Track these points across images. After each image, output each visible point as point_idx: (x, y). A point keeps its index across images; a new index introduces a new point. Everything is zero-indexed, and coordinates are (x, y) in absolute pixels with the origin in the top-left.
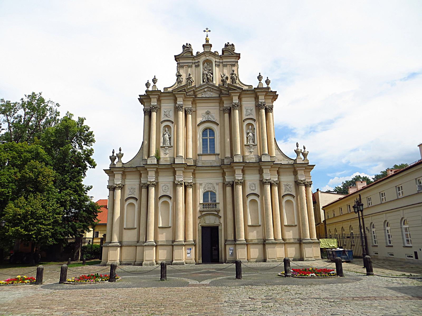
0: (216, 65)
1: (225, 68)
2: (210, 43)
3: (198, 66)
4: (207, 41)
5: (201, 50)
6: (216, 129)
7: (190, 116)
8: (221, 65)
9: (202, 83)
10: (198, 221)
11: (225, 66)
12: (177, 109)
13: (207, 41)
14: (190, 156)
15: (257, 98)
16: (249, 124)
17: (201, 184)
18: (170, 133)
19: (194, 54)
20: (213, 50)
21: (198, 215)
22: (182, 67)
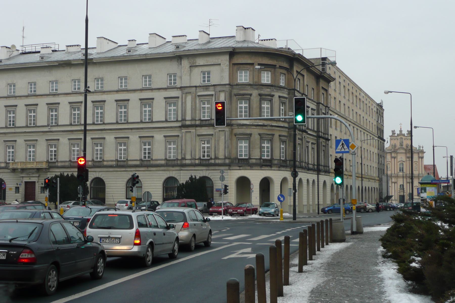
0: (405, 140)
1: (407, 141)
2: (402, 130)
3: (398, 140)
4: (401, 129)
5: (399, 133)
6: (404, 163)
7: (395, 159)
8: (406, 139)
9: (399, 146)
10: (398, 194)
11: (408, 140)
12: (392, 157)
13: (401, 128)
14: (396, 173)
15: (419, 154)
16: (416, 163)
17: (399, 182)
18: (389, 165)
19: (396, 135)
20: (403, 133)
21: (398, 192)
22: (392, 140)
